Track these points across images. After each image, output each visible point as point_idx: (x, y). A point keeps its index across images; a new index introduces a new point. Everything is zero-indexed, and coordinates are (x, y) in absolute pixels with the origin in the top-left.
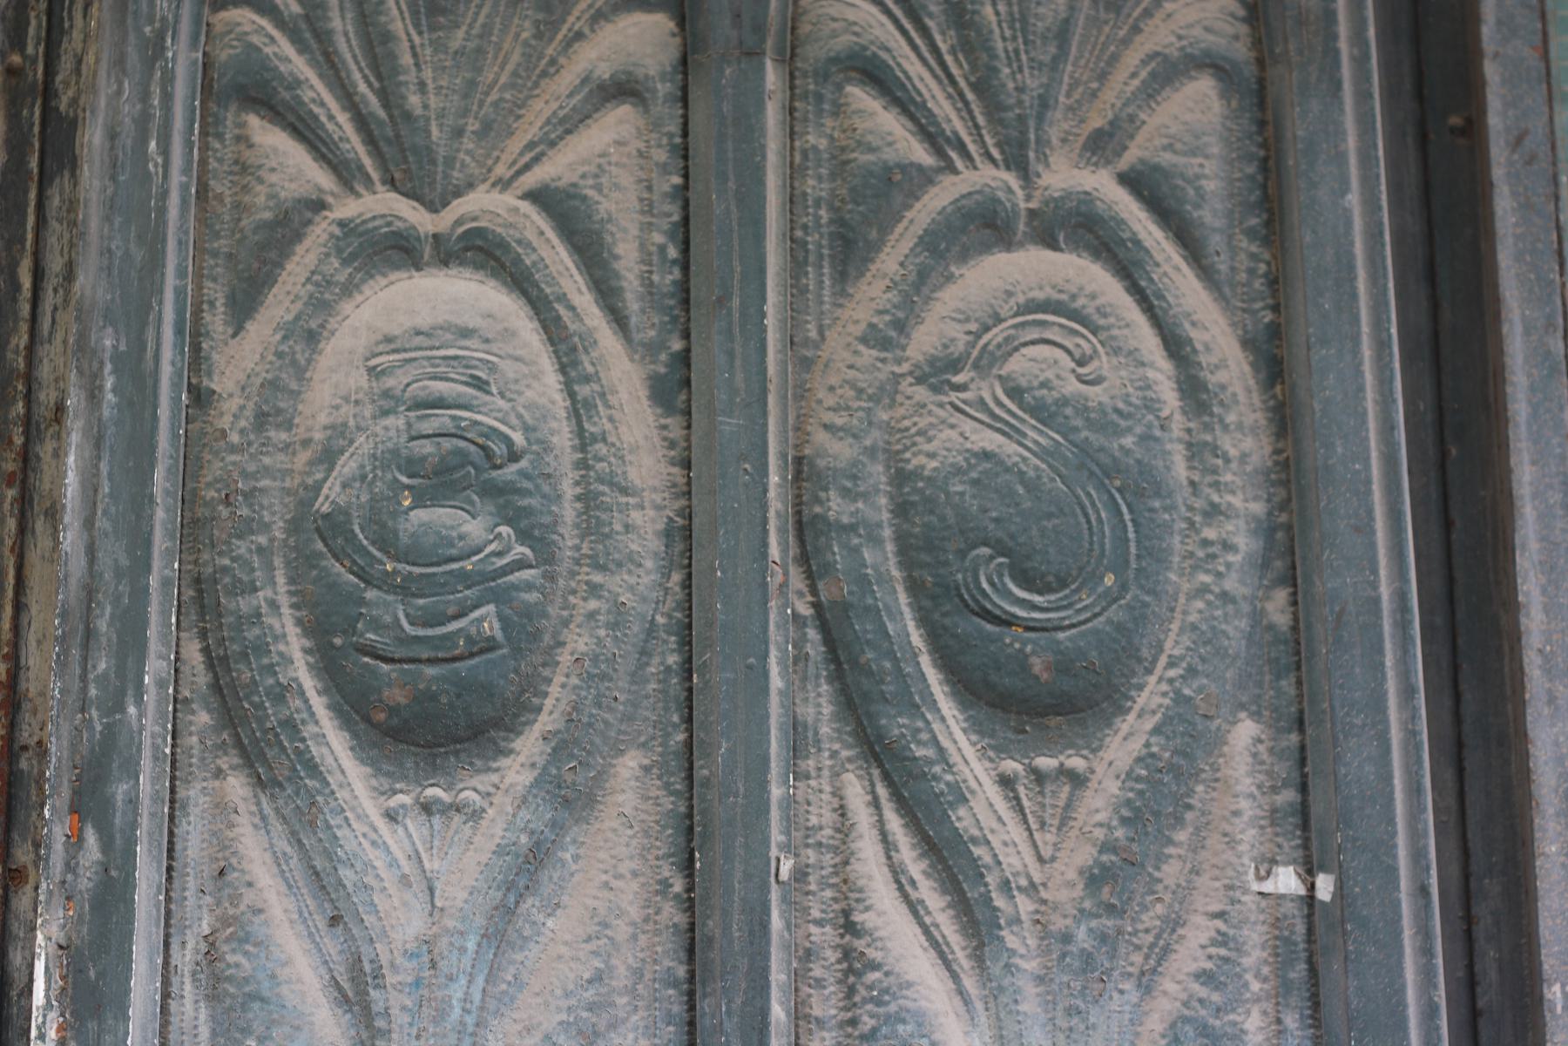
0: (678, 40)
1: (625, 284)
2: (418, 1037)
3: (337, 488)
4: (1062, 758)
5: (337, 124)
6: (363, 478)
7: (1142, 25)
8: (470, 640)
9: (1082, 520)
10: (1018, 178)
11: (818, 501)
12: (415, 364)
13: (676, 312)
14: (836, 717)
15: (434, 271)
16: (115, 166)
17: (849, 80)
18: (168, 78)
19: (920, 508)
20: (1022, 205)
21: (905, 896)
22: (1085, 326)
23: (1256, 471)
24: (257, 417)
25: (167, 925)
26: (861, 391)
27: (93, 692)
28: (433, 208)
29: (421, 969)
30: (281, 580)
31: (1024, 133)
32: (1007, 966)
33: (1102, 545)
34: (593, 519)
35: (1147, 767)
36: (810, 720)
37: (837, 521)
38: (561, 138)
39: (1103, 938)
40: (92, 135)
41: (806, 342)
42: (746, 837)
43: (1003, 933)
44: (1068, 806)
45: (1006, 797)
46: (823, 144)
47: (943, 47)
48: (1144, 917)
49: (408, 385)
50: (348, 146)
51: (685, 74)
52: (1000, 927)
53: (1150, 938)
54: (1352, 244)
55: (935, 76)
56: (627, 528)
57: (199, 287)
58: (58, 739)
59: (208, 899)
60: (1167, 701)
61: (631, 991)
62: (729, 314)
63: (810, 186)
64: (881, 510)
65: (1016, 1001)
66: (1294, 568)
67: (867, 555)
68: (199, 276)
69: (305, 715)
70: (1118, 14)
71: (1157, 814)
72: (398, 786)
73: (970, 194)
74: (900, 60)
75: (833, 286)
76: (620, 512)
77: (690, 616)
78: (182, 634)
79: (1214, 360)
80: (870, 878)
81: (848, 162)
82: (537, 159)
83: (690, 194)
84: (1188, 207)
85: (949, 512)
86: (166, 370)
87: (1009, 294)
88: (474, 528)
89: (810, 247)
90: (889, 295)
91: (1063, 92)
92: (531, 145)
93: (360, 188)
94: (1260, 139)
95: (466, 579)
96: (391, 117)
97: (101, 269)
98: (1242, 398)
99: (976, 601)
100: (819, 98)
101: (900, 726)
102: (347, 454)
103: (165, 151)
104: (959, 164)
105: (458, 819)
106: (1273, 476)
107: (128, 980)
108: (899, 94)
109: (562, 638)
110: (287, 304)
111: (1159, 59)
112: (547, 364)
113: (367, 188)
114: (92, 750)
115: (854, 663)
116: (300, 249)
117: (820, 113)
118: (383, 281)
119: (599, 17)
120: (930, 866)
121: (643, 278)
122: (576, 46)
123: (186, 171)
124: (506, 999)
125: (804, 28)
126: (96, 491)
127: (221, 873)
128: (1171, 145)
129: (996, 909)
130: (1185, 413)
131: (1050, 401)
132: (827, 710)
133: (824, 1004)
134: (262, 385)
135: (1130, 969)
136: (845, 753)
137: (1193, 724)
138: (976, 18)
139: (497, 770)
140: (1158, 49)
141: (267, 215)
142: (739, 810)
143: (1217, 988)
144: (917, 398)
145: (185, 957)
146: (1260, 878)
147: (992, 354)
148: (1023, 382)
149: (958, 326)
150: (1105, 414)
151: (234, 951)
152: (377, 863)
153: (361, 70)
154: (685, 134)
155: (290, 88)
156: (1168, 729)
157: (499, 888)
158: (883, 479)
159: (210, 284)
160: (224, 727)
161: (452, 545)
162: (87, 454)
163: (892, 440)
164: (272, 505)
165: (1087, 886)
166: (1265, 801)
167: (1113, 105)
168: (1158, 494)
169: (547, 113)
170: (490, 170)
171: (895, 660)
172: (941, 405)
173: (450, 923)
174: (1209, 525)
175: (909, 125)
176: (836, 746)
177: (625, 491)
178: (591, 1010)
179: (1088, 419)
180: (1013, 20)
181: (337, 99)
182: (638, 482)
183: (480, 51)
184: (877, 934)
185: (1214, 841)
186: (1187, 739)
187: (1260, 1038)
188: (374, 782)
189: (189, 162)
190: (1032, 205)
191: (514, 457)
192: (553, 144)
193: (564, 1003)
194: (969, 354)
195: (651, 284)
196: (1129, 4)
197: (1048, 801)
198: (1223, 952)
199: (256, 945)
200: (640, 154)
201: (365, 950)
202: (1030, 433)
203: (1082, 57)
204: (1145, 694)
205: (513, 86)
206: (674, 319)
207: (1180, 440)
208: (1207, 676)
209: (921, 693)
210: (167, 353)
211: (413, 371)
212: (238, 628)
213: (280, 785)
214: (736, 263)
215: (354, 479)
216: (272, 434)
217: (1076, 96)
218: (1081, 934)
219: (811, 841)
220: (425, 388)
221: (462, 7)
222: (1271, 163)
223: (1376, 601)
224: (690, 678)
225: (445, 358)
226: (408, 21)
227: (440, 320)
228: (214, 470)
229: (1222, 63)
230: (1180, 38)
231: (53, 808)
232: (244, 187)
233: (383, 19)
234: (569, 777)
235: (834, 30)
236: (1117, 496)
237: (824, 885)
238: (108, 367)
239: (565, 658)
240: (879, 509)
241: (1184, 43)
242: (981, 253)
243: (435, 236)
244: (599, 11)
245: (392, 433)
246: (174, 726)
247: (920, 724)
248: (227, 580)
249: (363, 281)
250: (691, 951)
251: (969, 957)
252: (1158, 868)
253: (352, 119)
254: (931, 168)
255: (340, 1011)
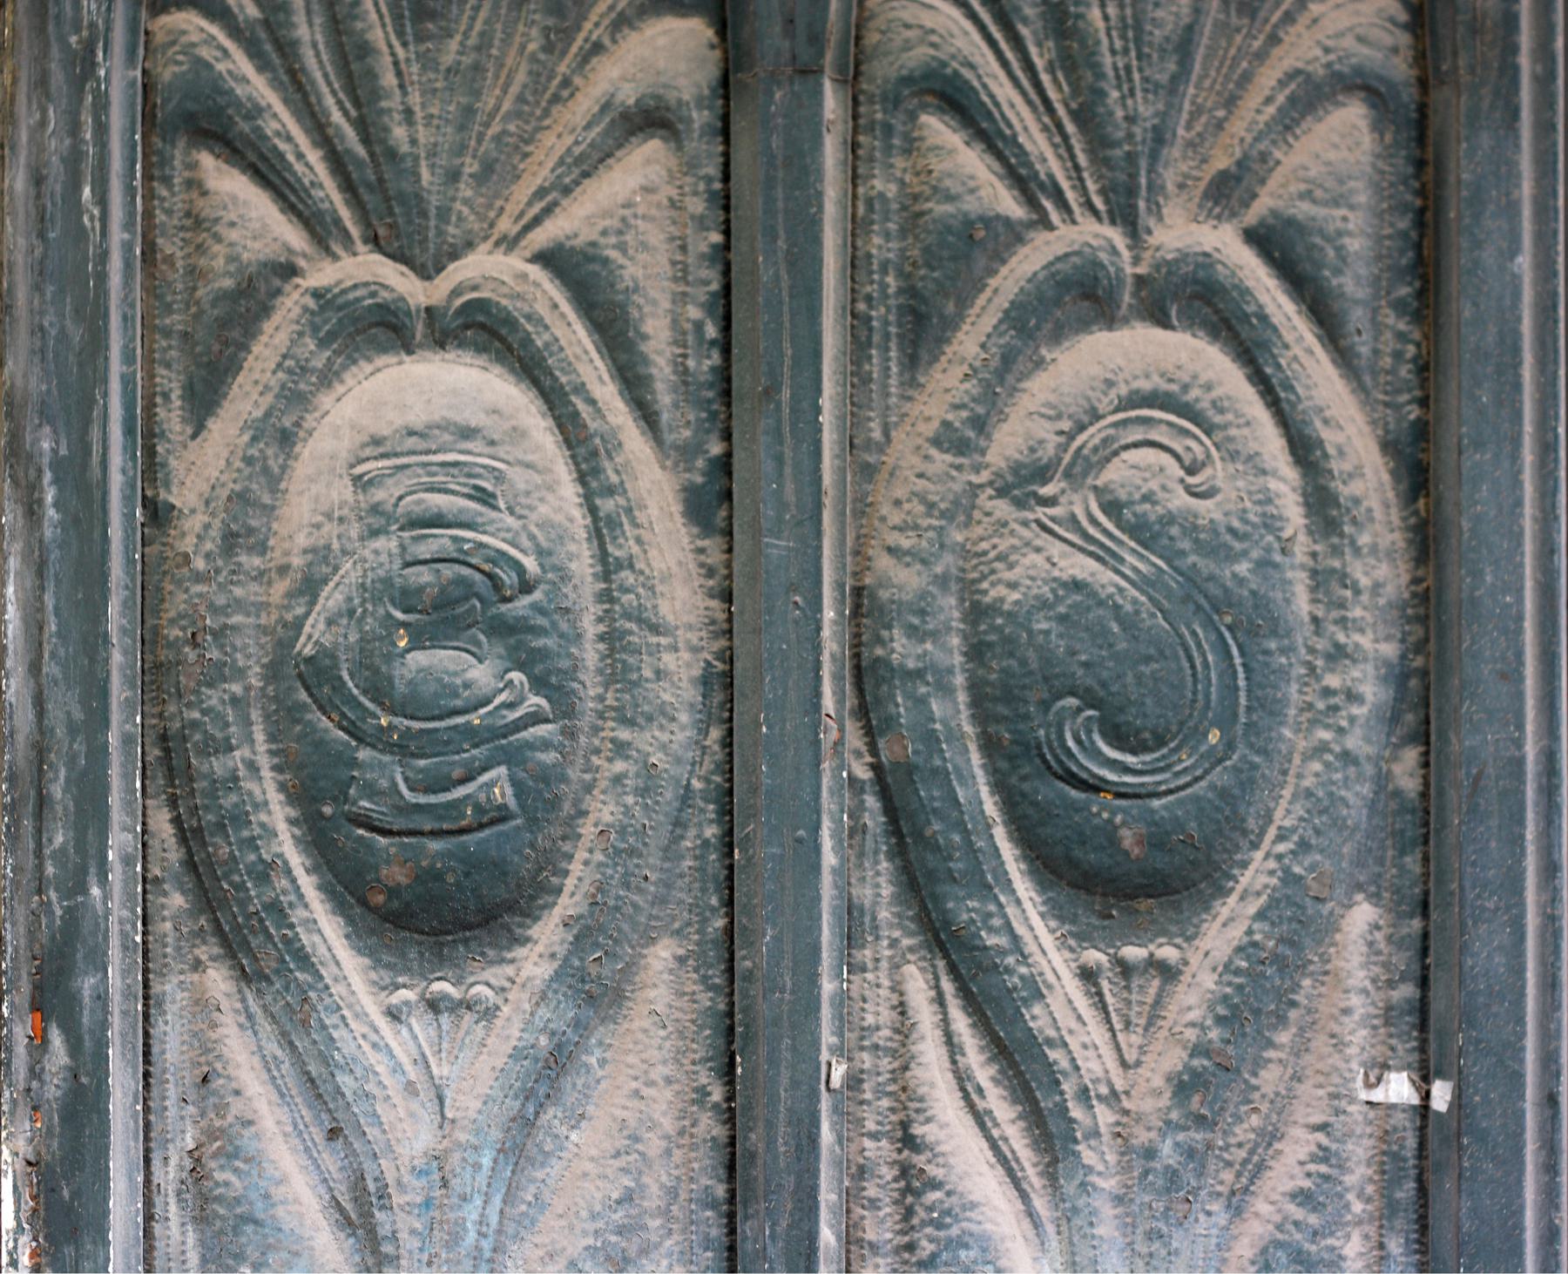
0: (717, 54)
1: (654, 371)
2: (429, 1264)
3: (321, 626)
4: (1152, 947)
5: (307, 165)
6: (351, 613)
7: (1281, 34)
8: (479, 809)
9: (1186, 665)
10: (1125, 234)
11: (879, 641)
12: (408, 472)
13: (715, 407)
14: (897, 899)
15: (428, 354)
16: (42, 219)
17: (924, 107)
18: (101, 105)
19: (998, 650)
20: (1129, 270)
21: (971, 1106)
22: (1197, 424)
23: (1390, 604)
24: (224, 538)
25: (147, 1139)
26: (931, 506)
27: (50, 870)
28: (426, 272)
29: (431, 1188)
30: (260, 737)
31: (1133, 176)
32: (1083, 1184)
33: (1207, 695)
34: (618, 673)
35: (1248, 958)
36: (867, 903)
37: (901, 665)
38: (577, 183)
39: (1190, 1153)
40: (13, 179)
41: (869, 445)
42: (793, 1039)
43: (1079, 1148)
44: (1157, 1003)
45: (1087, 993)
46: (892, 190)
47: (1039, 63)
48: (1237, 1130)
49: (400, 498)
50: (321, 194)
51: (726, 98)
52: (1076, 1141)
53: (1243, 1154)
54: (1519, 319)
55: (1029, 102)
56: (659, 674)
57: (150, 376)
58: (13, 924)
59: (191, 1109)
60: (1274, 881)
61: (665, 1213)
62: (778, 408)
63: (878, 246)
64: (952, 652)
65: (1091, 1224)
66: (1427, 722)
67: (935, 706)
68: (149, 361)
69: (293, 898)
70: (1253, 18)
71: (1257, 1012)
72: (400, 980)
73: (1067, 255)
74: (986, 80)
75: (901, 374)
76: (650, 654)
77: (731, 780)
78: (149, 802)
79: (1347, 466)
80: (932, 1085)
81: (922, 214)
82: (548, 211)
83: (732, 256)
84: (1327, 273)
85: (1031, 654)
86: (116, 480)
87: (1110, 384)
88: (481, 674)
89: (875, 323)
90: (967, 385)
91: (1183, 122)
92: (541, 193)
93: (337, 248)
94: (1416, 185)
95: (473, 736)
96: (372, 154)
97: (33, 352)
98: (1378, 514)
99: (1060, 762)
100: (888, 130)
101: (969, 910)
102: (331, 584)
103: (102, 200)
104: (1055, 217)
105: (468, 1017)
106: (1410, 611)
107: (106, 1200)
108: (984, 125)
109: (584, 807)
110: (255, 396)
111: (1300, 79)
112: (563, 472)
113: (346, 248)
114: (53, 938)
115: (919, 836)
116: (268, 326)
117: (888, 149)
118: (368, 368)
119: (622, 23)
120: (1001, 1072)
121: (676, 364)
122: (595, 60)
123: (129, 225)
124: (527, 1222)
125: (872, 38)
126: (41, 628)
127: (205, 1080)
128: (1310, 192)
129: (1072, 1121)
130: (1310, 533)
131: (1153, 518)
132: (887, 891)
133: (880, 1228)
134: (229, 499)
135: (1219, 1188)
136: (907, 942)
137: (1302, 908)
138: (1081, 24)
139: (512, 961)
140: (1300, 65)
141: (228, 283)
142: (785, 1008)
143: (1314, 1210)
144: (998, 514)
145: (169, 1175)
146: (1369, 1086)
147: (1086, 459)
148: (1122, 495)
149: (1047, 425)
150: (1216, 532)
151: (222, 1167)
152: (379, 1069)
153: (334, 92)
154: (726, 178)
155: (249, 117)
156: (1273, 914)
157: (516, 1097)
158: (956, 614)
159: (164, 372)
160: (201, 912)
161: (456, 695)
162: (28, 584)
163: (968, 566)
164: (246, 646)
165: (1175, 1094)
166: (1378, 997)
167: (1242, 140)
168: (1274, 633)
169: (560, 150)
170: (492, 225)
171: (966, 833)
172: (1025, 524)
173: (462, 1137)
174: (1332, 671)
175: (996, 166)
176: (897, 934)
177: (655, 629)
178: (620, 1233)
179: (1196, 541)
180: (1125, 27)
181: (307, 131)
182: (670, 618)
183: (477, 68)
184: (938, 1149)
185: (1320, 1043)
186: (1294, 925)
187: (1360, 1264)
188: (373, 975)
189: (131, 214)
190: (1140, 270)
191: (526, 587)
192: (567, 191)
193: (590, 1226)
194: (1060, 460)
195: (686, 371)
196: (1267, 6)
197: (1134, 997)
198: (1323, 1169)
199: (247, 1161)
200: (673, 204)
201: (369, 1168)
202: (1129, 558)
203: (1206, 76)
204: (1249, 873)
205: (518, 114)
206: (713, 416)
207: (1303, 567)
208: (1322, 851)
209: (994, 871)
210: (116, 459)
211: (406, 481)
212: (212, 794)
213: (267, 979)
214: (786, 345)
215: (340, 615)
216: (243, 559)
217: (1198, 128)
218: (1166, 1148)
219: (866, 1043)
220: (419, 502)
221: (454, 9)
222: (1429, 215)
223: (1520, 762)
224: (731, 854)
225: (443, 464)
226: (390, 29)
227: (436, 417)
228: (177, 603)
229: (1375, 83)
230: (1327, 50)
231: (12, 1005)
232: (199, 247)
233: (359, 25)
234: (594, 970)
235: (907, 41)
236: (1227, 635)
237: (880, 1092)
238: (48, 476)
239: (588, 830)
240: (951, 652)
241: (1332, 57)
242: (1077, 332)
243: (428, 310)
244: (621, 14)
245: (384, 558)
246: (144, 909)
247: (992, 908)
248: (198, 737)
249: (345, 367)
250: (731, 1168)
251: (1041, 1174)
252: (1255, 1074)
253: (325, 158)
254: (1021, 222)
255: (342, 1235)
